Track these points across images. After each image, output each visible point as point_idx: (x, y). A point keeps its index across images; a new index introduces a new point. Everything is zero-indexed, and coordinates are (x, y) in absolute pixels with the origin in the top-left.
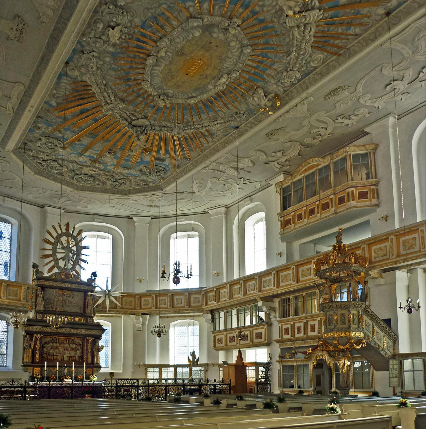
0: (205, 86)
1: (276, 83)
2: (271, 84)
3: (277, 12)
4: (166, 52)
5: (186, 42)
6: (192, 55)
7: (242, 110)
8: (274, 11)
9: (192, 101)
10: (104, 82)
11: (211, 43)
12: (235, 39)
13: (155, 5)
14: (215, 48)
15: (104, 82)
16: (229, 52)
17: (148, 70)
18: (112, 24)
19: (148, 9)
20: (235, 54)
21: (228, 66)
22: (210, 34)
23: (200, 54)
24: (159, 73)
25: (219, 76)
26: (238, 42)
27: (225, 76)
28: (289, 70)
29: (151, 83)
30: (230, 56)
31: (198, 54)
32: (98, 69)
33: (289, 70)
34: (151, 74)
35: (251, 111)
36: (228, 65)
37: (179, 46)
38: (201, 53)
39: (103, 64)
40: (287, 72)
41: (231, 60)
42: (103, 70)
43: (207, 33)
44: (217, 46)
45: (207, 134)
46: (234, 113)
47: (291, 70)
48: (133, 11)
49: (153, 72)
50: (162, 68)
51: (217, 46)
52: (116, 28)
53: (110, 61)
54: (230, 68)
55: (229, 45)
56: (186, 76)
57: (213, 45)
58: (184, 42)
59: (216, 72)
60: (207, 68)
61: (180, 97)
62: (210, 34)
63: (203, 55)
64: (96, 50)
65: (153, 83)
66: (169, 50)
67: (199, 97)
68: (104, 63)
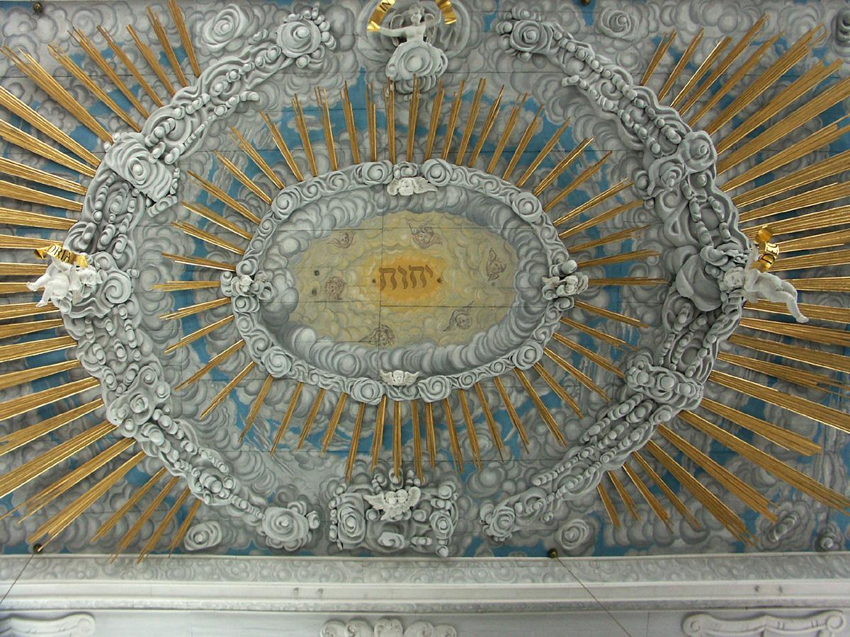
0: (455, 211)
1: (351, 48)
2: (359, 57)
3: (161, 224)
4: (394, 369)
5: (343, 343)
6: (372, 307)
7: (498, 48)
8: (165, 233)
9: (529, 205)
10: (572, 452)
11: (314, 292)
12: (275, 250)
13: (288, 456)
14: (323, 272)
15: (572, 452)
16: (318, 233)
17: (482, 372)
18: (372, 516)
19: (301, 462)
20: (313, 218)
21: (360, 203)
22: (294, 307)
23: (361, 292)
24: (472, 345)
25: (402, 202)
26: (279, 239)
27: (391, 191)
28: (288, 62)
29: (518, 346)
30: (327, 224)
31: (361, 297)
32: (530, 486)
33: (288, 62)
34: (483, 361)
35: (488, 20)
36: (355, 209)
37: (361, 352)
38: (354, 292)
39: (512, 480)
40: (296, 59)
41: (337, 214)
42: (531, 472)
43: (294, 317)
44: (317, 273)
45: (667, 59)
46: (523, 61)
47: (286, 58)
48: (324, 486)
49: (473, 360)
50: (450, 348)
51: (317, 273)
52: (377, 507)
53: (494, 470)
54: (365, 195)
55: (299, 250)
56: (445, 279)
57: (316, 284)
58: (346, 347)
59: (392, 220)
60: (391, 248)
61: (534, 244)
62: (294, 307)
63: (358, 284)
64: (473, 512)
65: (516, 340)
66: (387, 366)
67: (506, 200)
68: (506, 479)
